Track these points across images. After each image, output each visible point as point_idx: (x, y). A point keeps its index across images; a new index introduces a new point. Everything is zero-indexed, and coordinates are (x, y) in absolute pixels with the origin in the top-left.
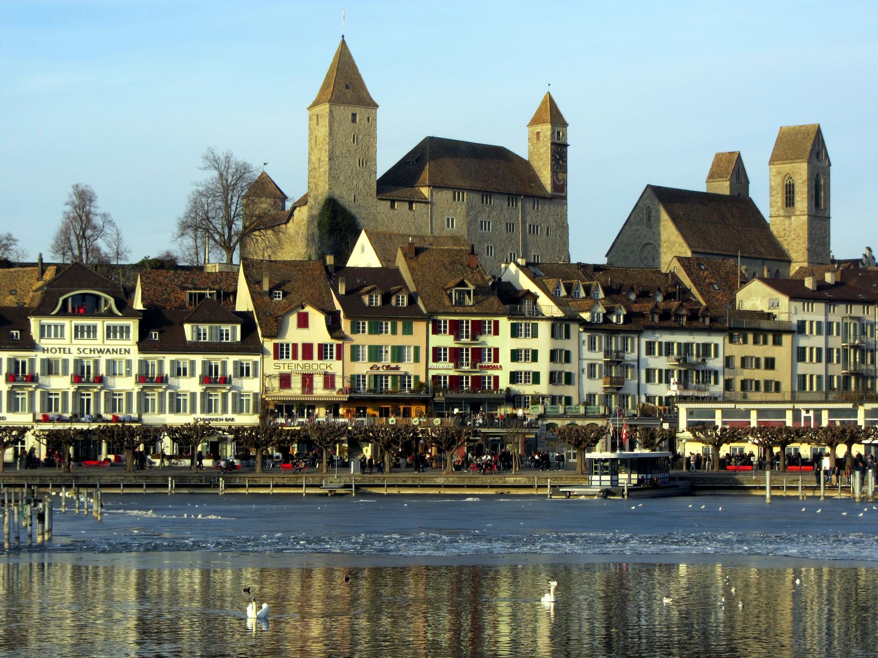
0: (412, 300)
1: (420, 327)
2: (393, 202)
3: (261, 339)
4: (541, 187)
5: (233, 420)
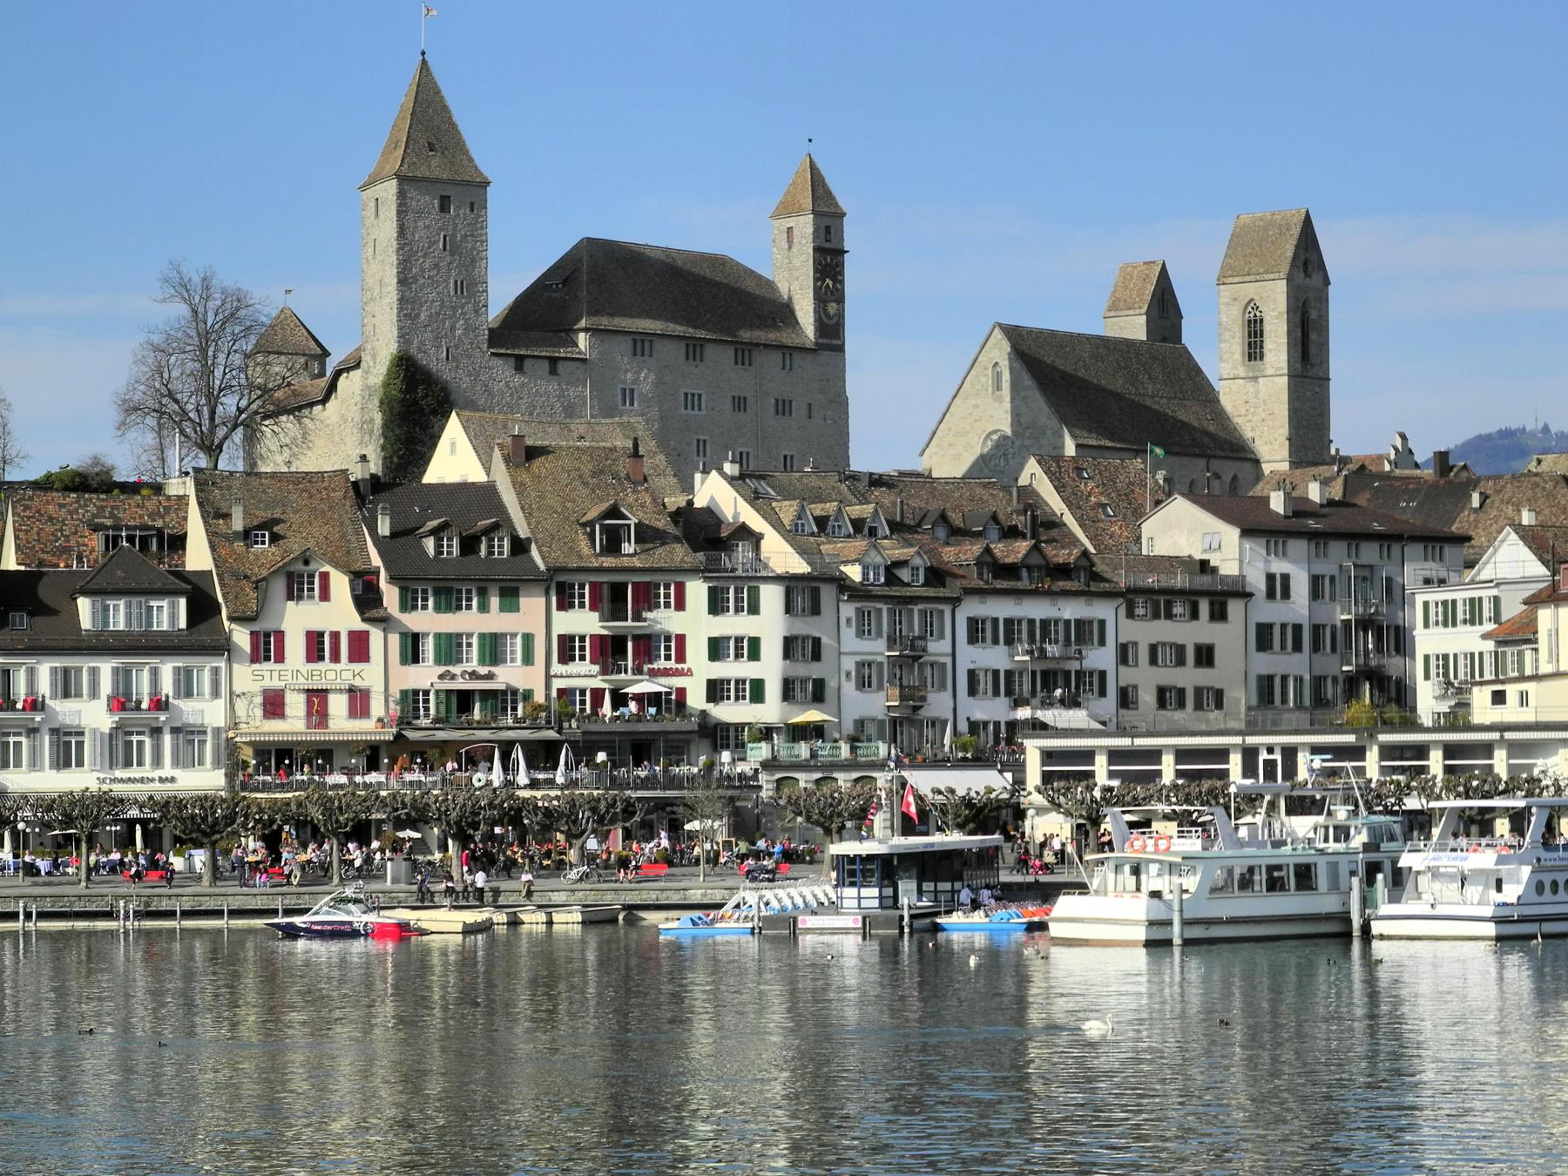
3: (226, 623)
5: (173, 780)
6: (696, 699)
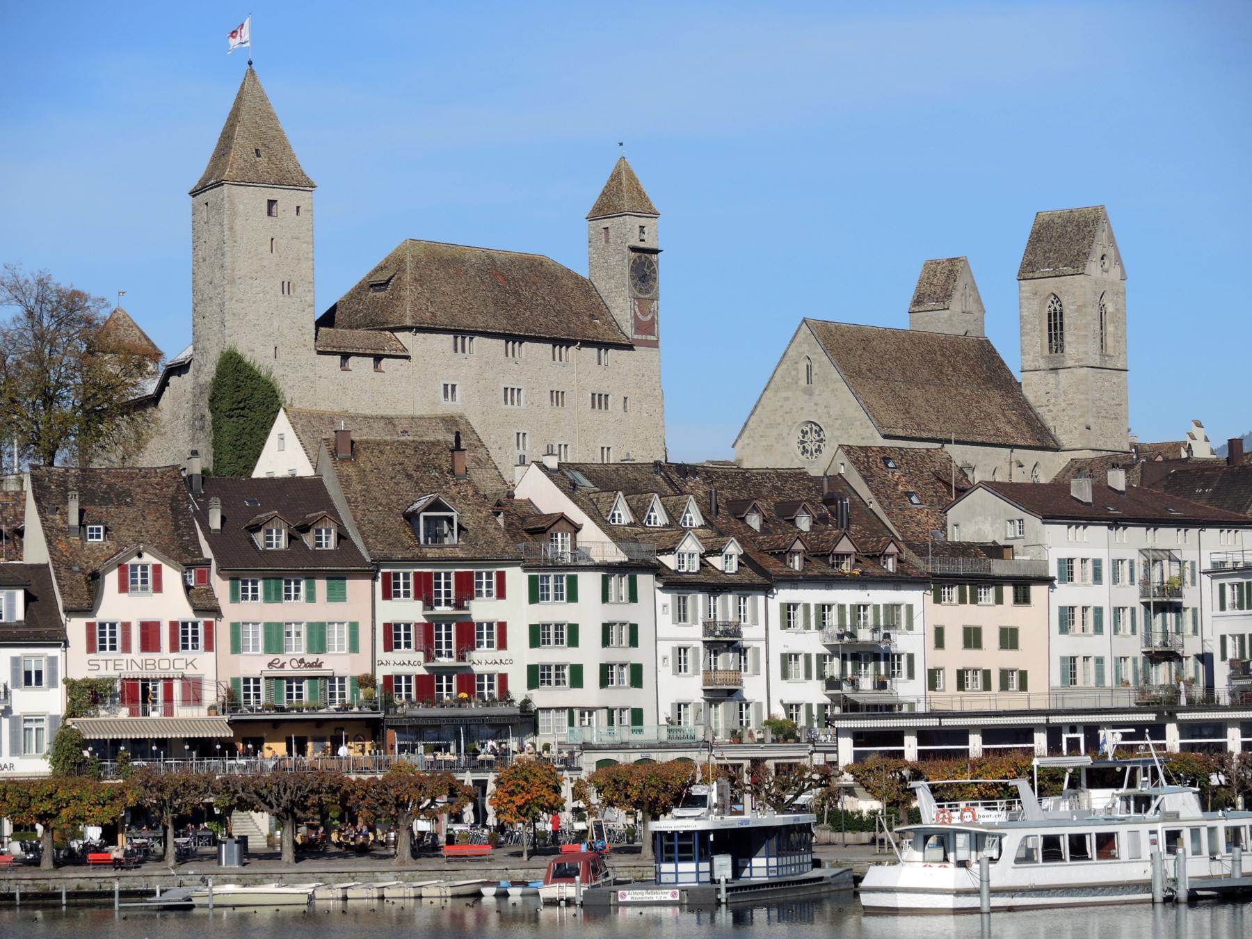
0: (342, 537)
1: (358, 589)
2: (345, 356)
3: (63, 616)
4: (613, 325)
5: (12, 766)
6: (518, 689)
